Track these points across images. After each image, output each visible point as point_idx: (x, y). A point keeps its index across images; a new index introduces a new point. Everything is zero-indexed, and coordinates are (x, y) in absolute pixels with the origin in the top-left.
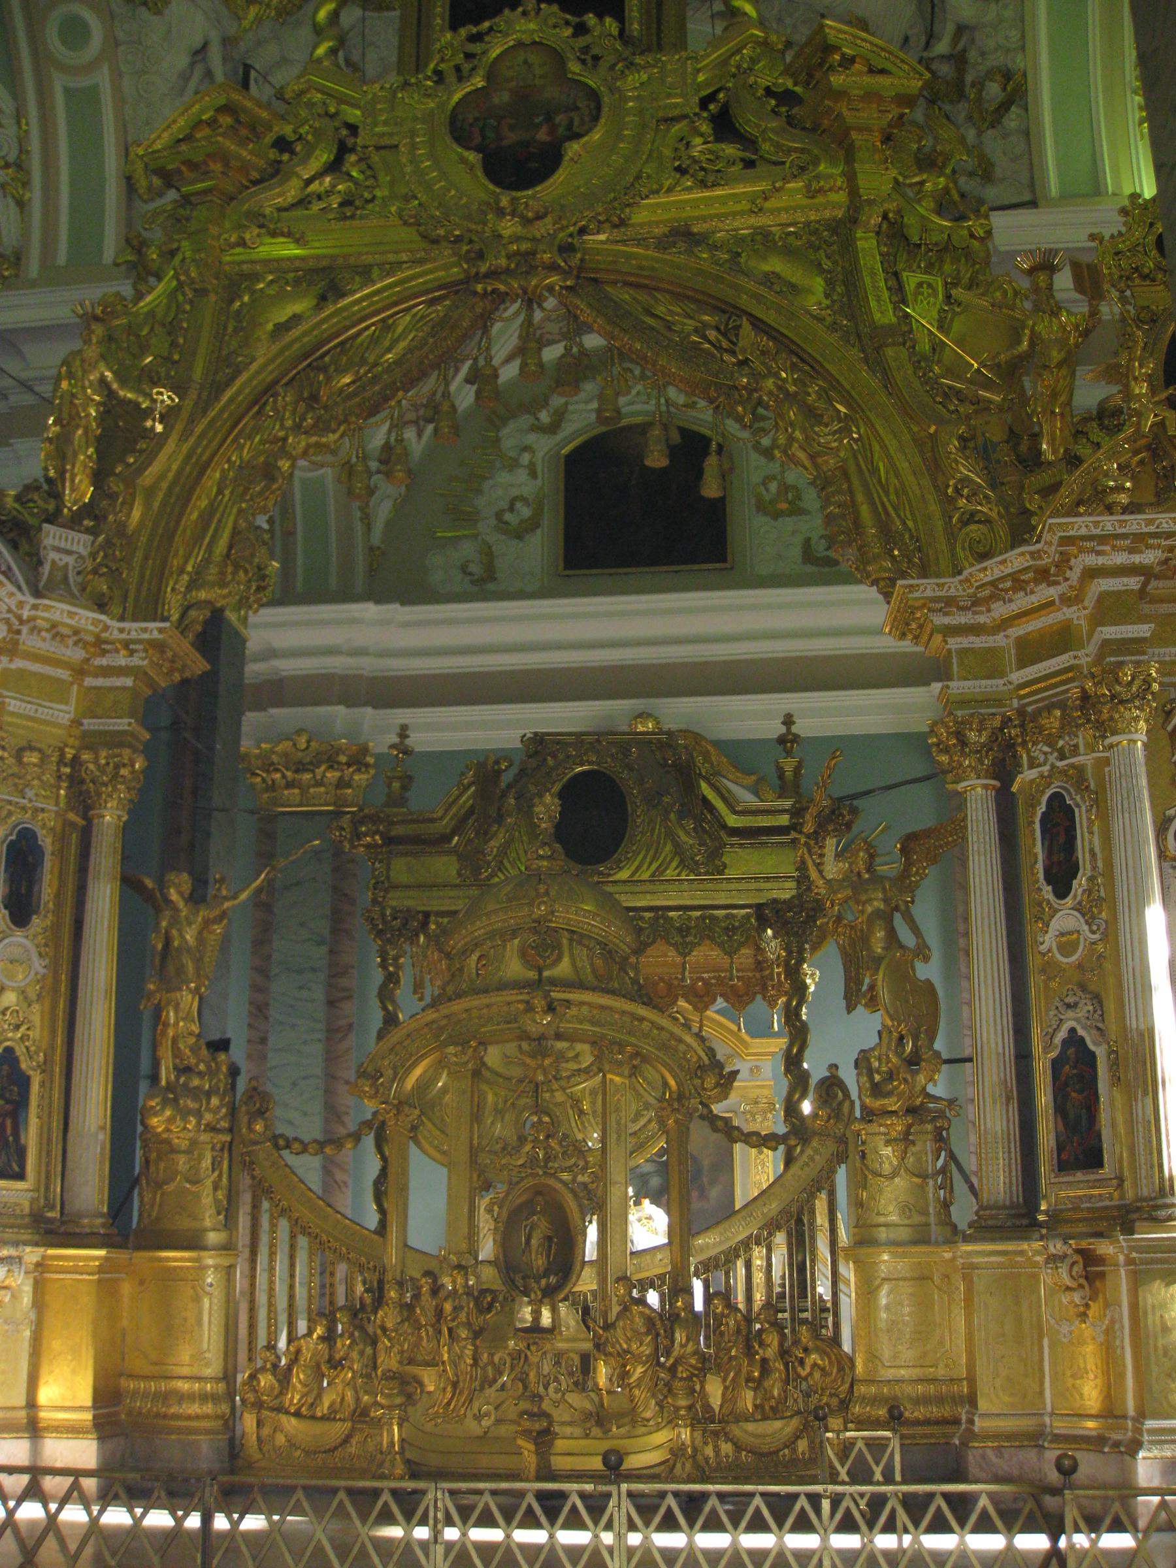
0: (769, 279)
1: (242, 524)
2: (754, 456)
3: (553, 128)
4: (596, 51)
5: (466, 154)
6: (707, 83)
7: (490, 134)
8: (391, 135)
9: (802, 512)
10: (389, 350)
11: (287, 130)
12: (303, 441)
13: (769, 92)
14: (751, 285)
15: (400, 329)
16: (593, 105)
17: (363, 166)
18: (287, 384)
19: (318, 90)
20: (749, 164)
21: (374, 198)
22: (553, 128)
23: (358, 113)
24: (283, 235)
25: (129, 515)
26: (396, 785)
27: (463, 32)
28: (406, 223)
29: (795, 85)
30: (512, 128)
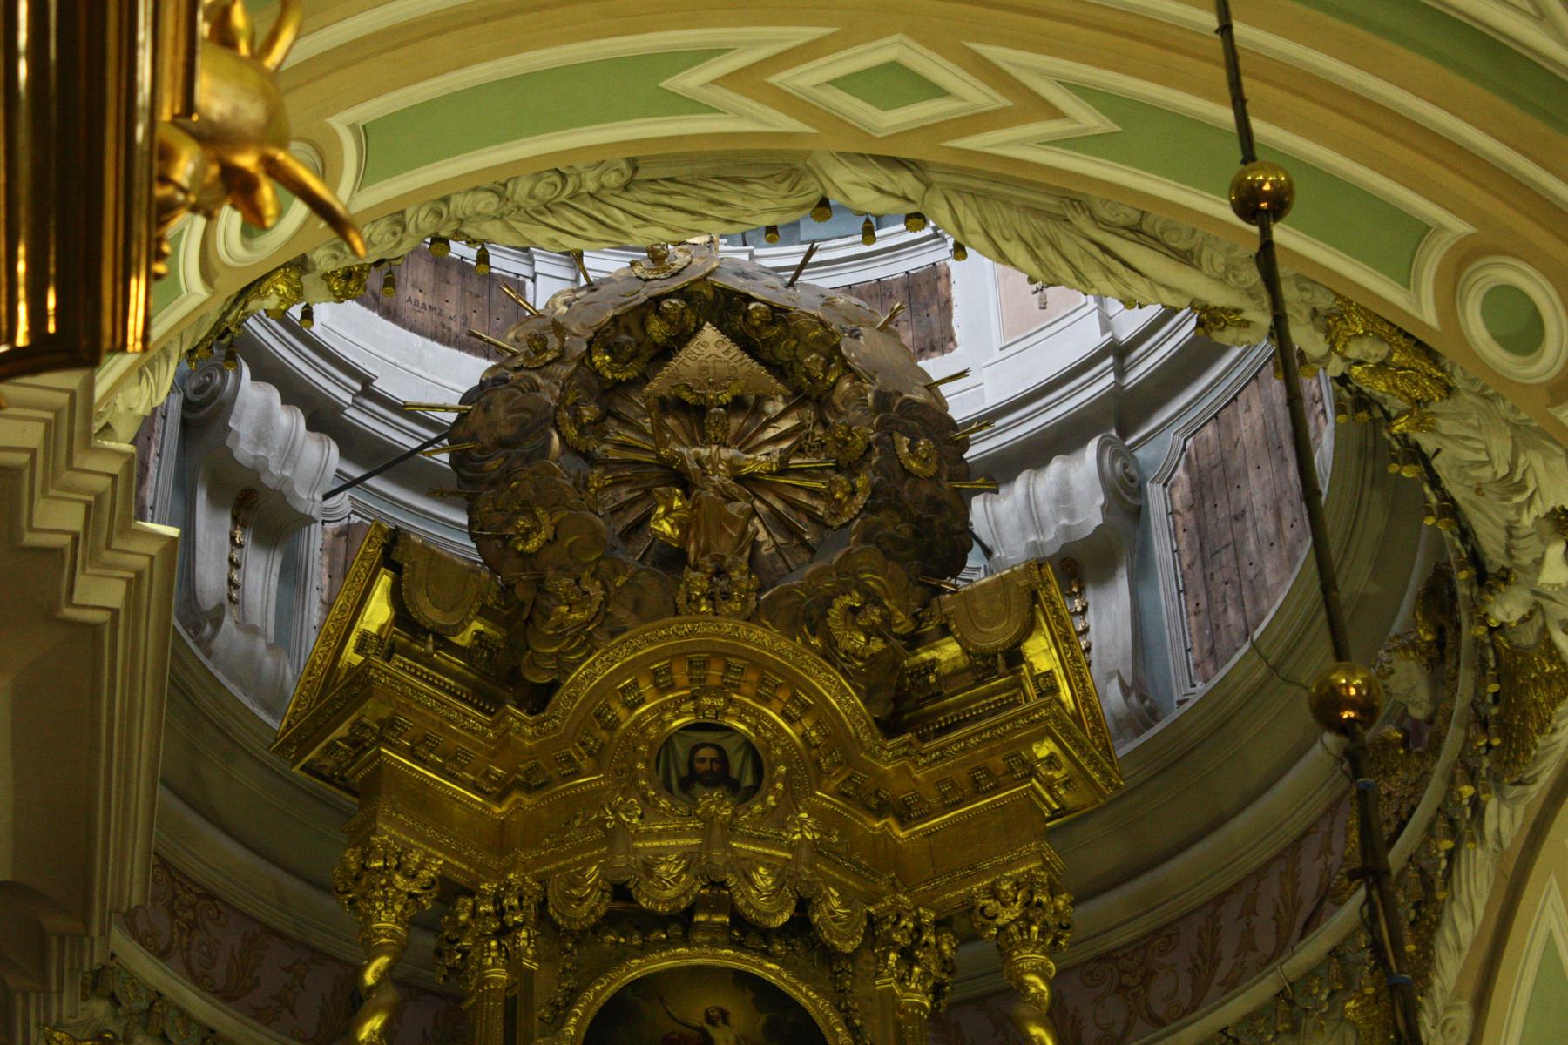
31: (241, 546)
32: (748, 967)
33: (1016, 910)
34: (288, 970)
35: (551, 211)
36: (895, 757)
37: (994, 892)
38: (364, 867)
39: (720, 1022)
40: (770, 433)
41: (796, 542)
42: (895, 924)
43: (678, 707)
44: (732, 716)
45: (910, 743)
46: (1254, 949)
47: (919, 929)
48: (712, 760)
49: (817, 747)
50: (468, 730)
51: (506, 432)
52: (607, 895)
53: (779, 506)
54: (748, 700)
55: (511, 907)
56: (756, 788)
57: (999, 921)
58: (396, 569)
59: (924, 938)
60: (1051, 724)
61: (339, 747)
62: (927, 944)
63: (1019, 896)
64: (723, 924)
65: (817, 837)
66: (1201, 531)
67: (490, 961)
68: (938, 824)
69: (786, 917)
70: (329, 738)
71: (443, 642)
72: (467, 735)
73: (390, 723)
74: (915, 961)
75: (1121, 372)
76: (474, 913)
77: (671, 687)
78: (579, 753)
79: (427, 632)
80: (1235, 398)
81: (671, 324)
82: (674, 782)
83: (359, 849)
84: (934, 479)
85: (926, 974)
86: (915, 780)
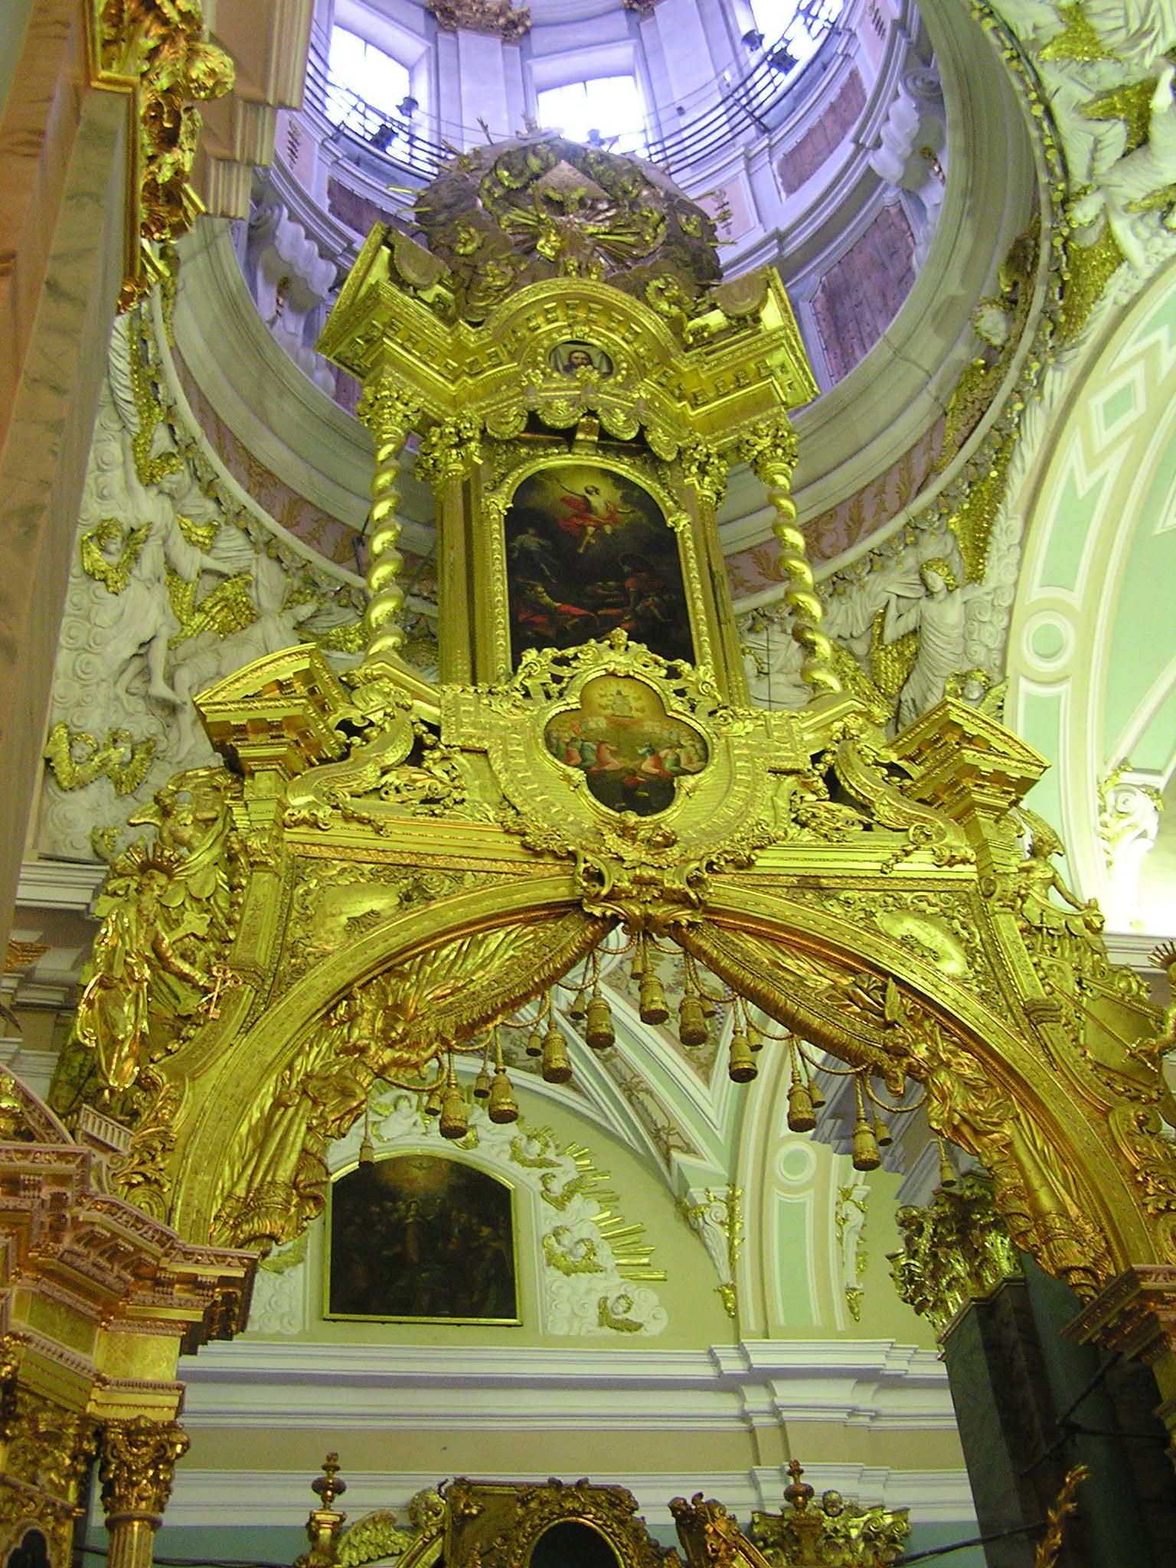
0: (907, 942)
1: (313, 1146)
2: (543, 1204)
5: (571, 770)
6: (810, 745)
7: (592, 757)
8: (480, 739)
9: (597, 1269)
10: (482, 966)
11: (355, 717)
12: (388, 1055)
13: (877, 763)
14: (891, 947)
15: (493, 947)
16: (698, 746)
18: (362, 987)
19: (391, 680)
20: (868, 828)
21: (463, 800)
22: (659, 762)
24: (361, 821)
25: (173, 1114)
26: (325, 1533)
27: (551, 652)
28: (507, 832)
30: (614, 753)
33: (766, 442)
37: (755, 432)
40: (601, 217)
46: (885, 510)
47: (708, 456)
51: (449, 201)
57: (759, 448)
58: (391, 247)
66: (835, 319)
69: (633, 434)
75: (781, 249)
77: (556, 321)
79: (409, 285)
82: (561, 367)
84: (701, 238)
85: (712, 483)
86: (700, 379)
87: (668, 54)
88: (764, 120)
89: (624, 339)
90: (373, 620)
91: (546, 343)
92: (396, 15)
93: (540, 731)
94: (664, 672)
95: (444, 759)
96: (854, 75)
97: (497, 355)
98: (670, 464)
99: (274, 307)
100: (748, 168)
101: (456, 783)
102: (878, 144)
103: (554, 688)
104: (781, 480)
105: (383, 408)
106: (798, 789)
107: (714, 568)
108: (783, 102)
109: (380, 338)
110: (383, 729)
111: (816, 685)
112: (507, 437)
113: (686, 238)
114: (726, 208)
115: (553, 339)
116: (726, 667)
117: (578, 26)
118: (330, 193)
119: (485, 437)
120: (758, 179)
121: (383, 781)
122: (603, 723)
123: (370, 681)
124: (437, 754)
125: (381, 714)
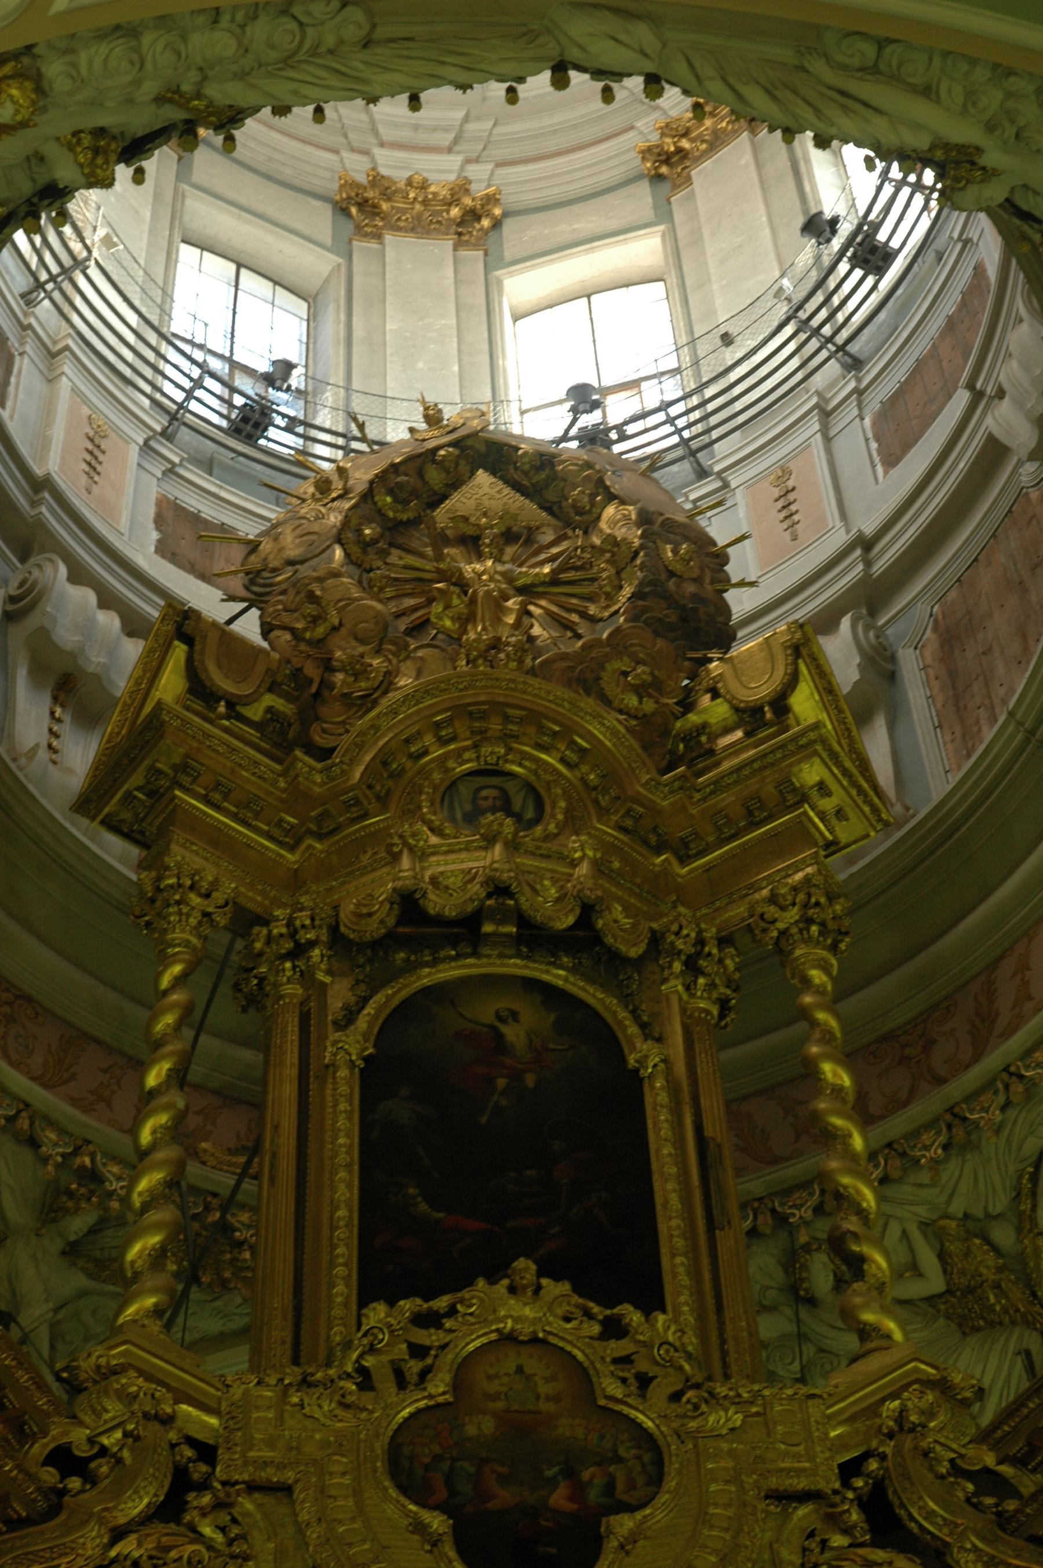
3: (579, 1490)
4: (643, 1365)
6: (842, 1443)
8: (281, 1467)
11: (78, 1436)
13: (956, 1469)
16: (647, 1457)
17: (224, 1518)
19: (141, 1373)
22: (579, 1490)
23: (213, 1421)
27: (407, 1306)
29: (1000, 1462)
31: (59, 721)
32: (537, 975)
33: (794, 914)
34: (105, 1071)
35: (292, 67)
36: (671, 792)
38: (158, 890)
39: (510, 1020)
41: (569, 634)
42: (677, 934)
43: (460, 755)
44: (512, 762)
45: (682, 777)
46: (1031, 998)
48: (495, 798)
49: (595, 788)
50: (260, 777)
51: (293, 553)
52: (396, 906)
53: (554, 609)
54: (527, 749)
55: (303, 926)
56: (538, 820)
57: (781, 925)
58: (188, 640)
59: (707, 949)
60: (819, 748)
61: (135, 797)
62: (709, 954)
63: (798, 900)
64: (508, 935)
65: (599, 855)
66: (953, 675)
67: (285, 979)
68: (715, 859)
69: (570, 920)
70: (126, 787)
71: (233, 713)
72: (259, 781)
73: (183, 767)
74: (699, 972)
75: (868, 564)
76: (269, 940)
77: (453, 739)
78: (367, 797)
80: (976, 560)
81: (448, 472)
82: (459, 815)
83: (154, 874)
84: (698, 580)
85: (711, 986)
87: (712, 248)
88: (854, 348)
89: (563, 760)
90: (127, 1266)
91: (437, 776)
92: (284, 218)
93: (380, 1446)
94: (596, 1329)
95: (220, 1505)
96: (979, 270)
97: (357, 802)
98: (638, 963)
99: (46, 720)
100: (824, 430)
101: (236, 1549)
102: (1001, 394)
103: (414, 1367)
104: (817, 976)
105: (168, 906)
106: (819, 1525)
107: (708, 1132)
108: (882, 315)
109: (170, 789)
110: (120, 1461)
111: (865, 1332)
112: (368, 937)
113: (671, 584)
114: (791, 497)
115: (447, 771)
116: (719, 1308)
117: (576, 208)
118: (159, 521)
119: (337, 940)
120: (840, 445)
121: (113, 1553)
122: (488, 1425)
123: (105, 1377)
124: (206, 1499)
125: (118, 1434)
